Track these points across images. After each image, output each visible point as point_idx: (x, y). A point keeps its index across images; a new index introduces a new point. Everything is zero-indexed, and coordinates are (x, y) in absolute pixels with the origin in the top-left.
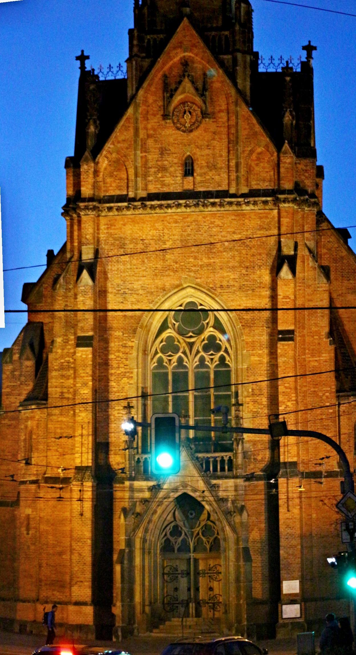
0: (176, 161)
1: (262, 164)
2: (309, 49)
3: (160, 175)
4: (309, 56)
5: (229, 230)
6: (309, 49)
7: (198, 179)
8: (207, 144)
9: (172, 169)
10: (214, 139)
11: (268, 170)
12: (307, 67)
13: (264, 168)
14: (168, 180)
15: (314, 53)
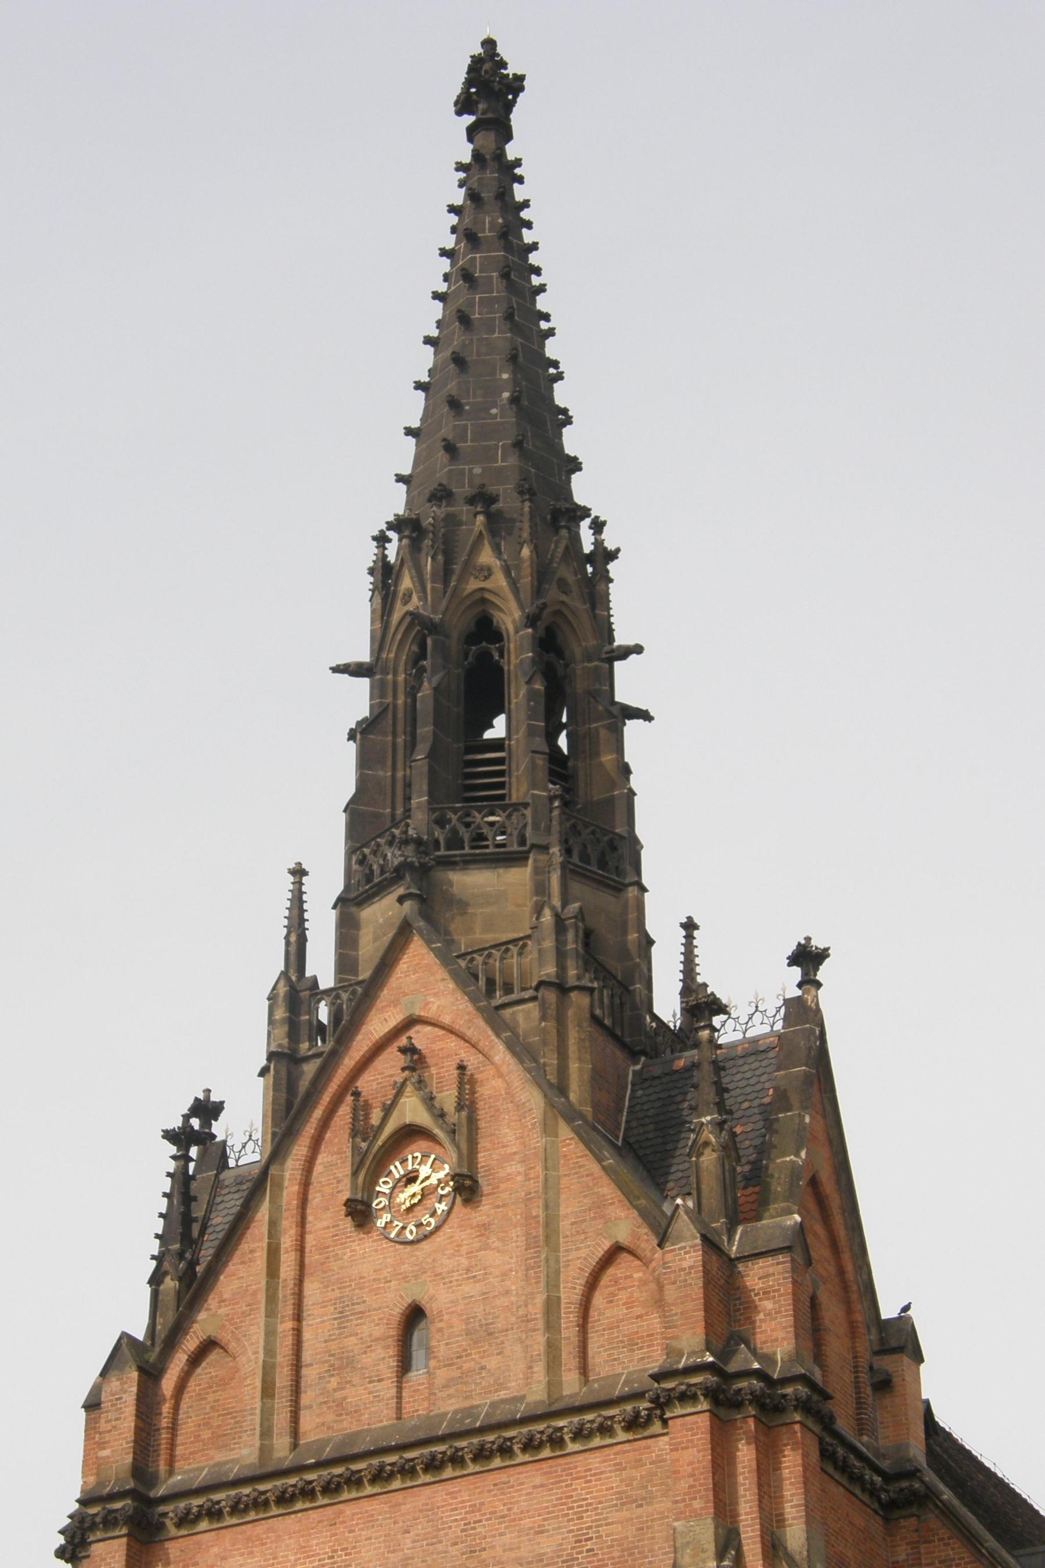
0: (379, 1331)
1: (623, 1296)
2: (808, 958)
3: (334, 1382)
4: (810, 982)
5: (526, 1523)
6: (808, 958)
7: (442, 1375)
8: (465, 1262)
9: (367, 1360)
10: (486, 1247)
11: (638, 1310)
12: (803, 1014)
13: (629, 1305)
14: (356, 1394)
15: (823, 974)
